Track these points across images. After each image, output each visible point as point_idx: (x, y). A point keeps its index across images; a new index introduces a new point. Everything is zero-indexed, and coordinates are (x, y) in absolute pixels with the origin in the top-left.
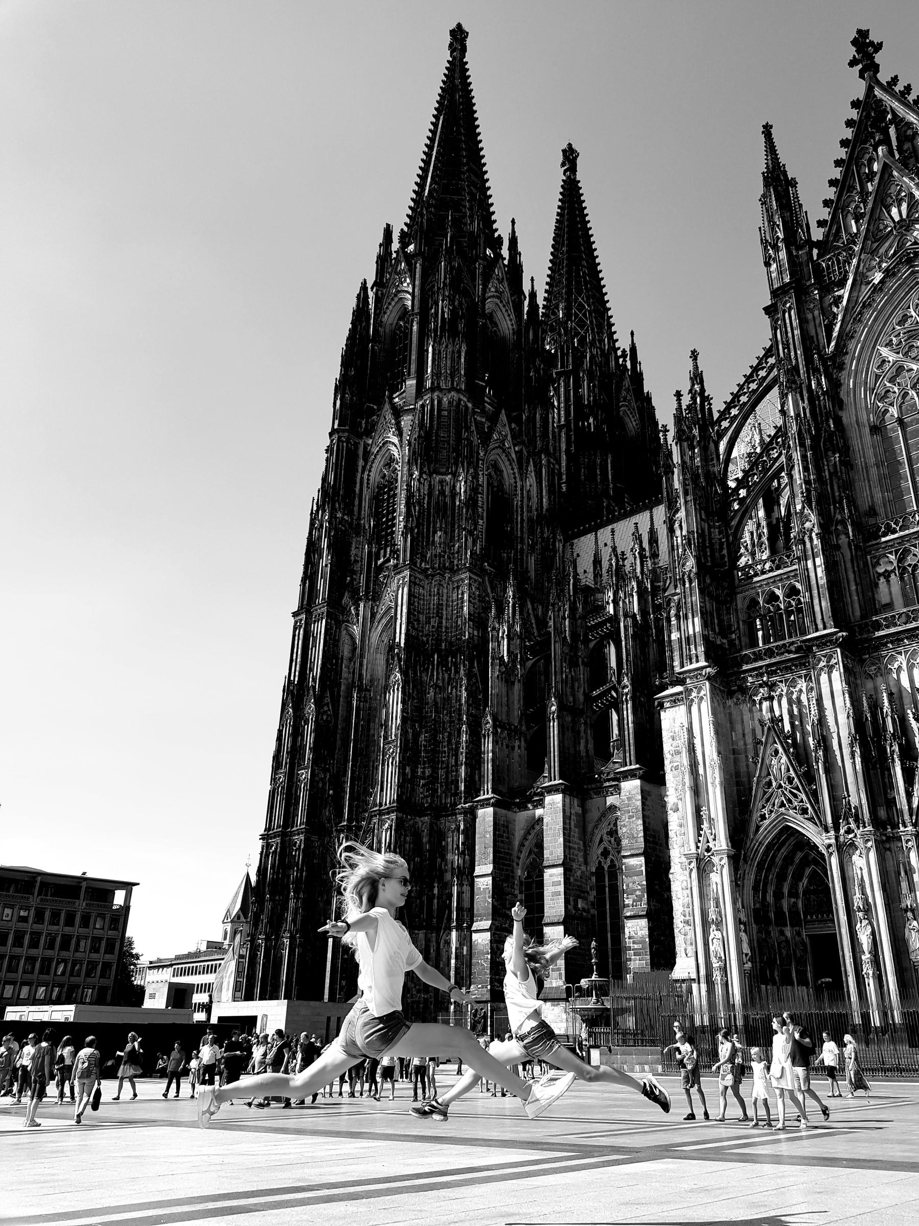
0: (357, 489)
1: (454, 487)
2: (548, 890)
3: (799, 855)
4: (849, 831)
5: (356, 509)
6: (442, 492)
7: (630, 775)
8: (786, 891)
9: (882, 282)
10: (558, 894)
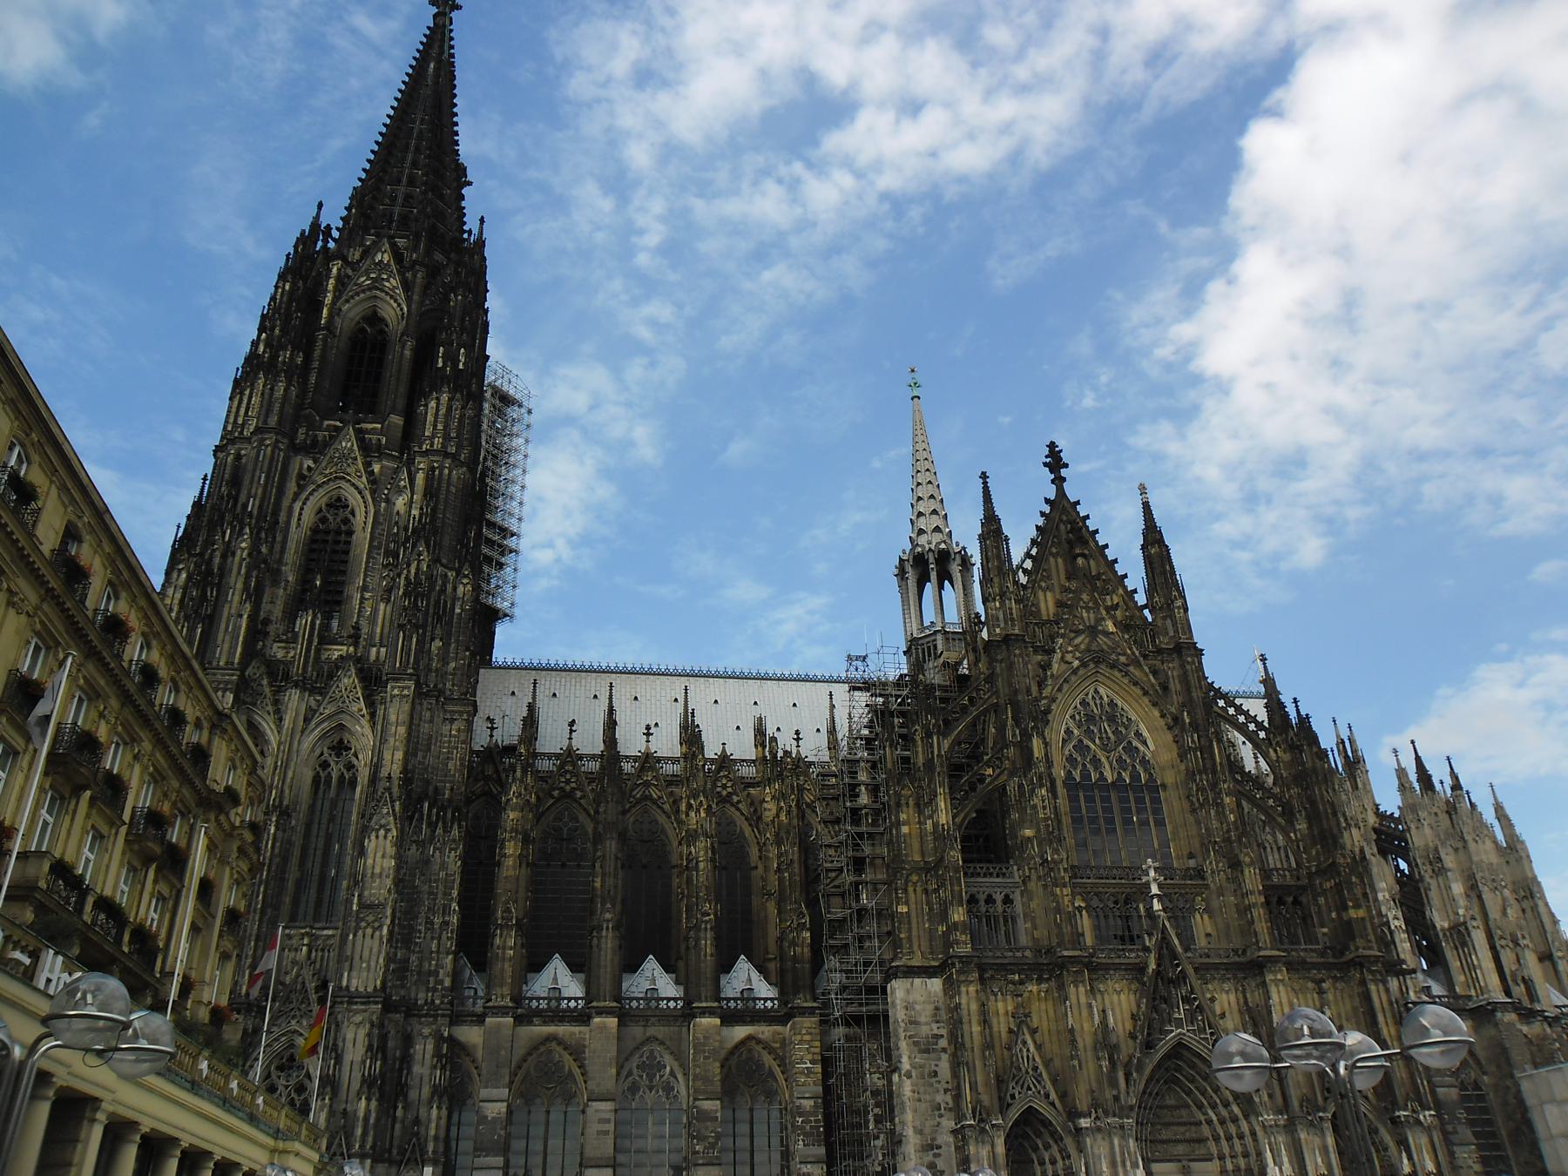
0: (282, 518)
1: (455, 589)
2: (593, 1128)
4: (1097, 1118)
5: (277, 547)
6: (443, 591)
7: (711, 1012)
10: (606, 1133)
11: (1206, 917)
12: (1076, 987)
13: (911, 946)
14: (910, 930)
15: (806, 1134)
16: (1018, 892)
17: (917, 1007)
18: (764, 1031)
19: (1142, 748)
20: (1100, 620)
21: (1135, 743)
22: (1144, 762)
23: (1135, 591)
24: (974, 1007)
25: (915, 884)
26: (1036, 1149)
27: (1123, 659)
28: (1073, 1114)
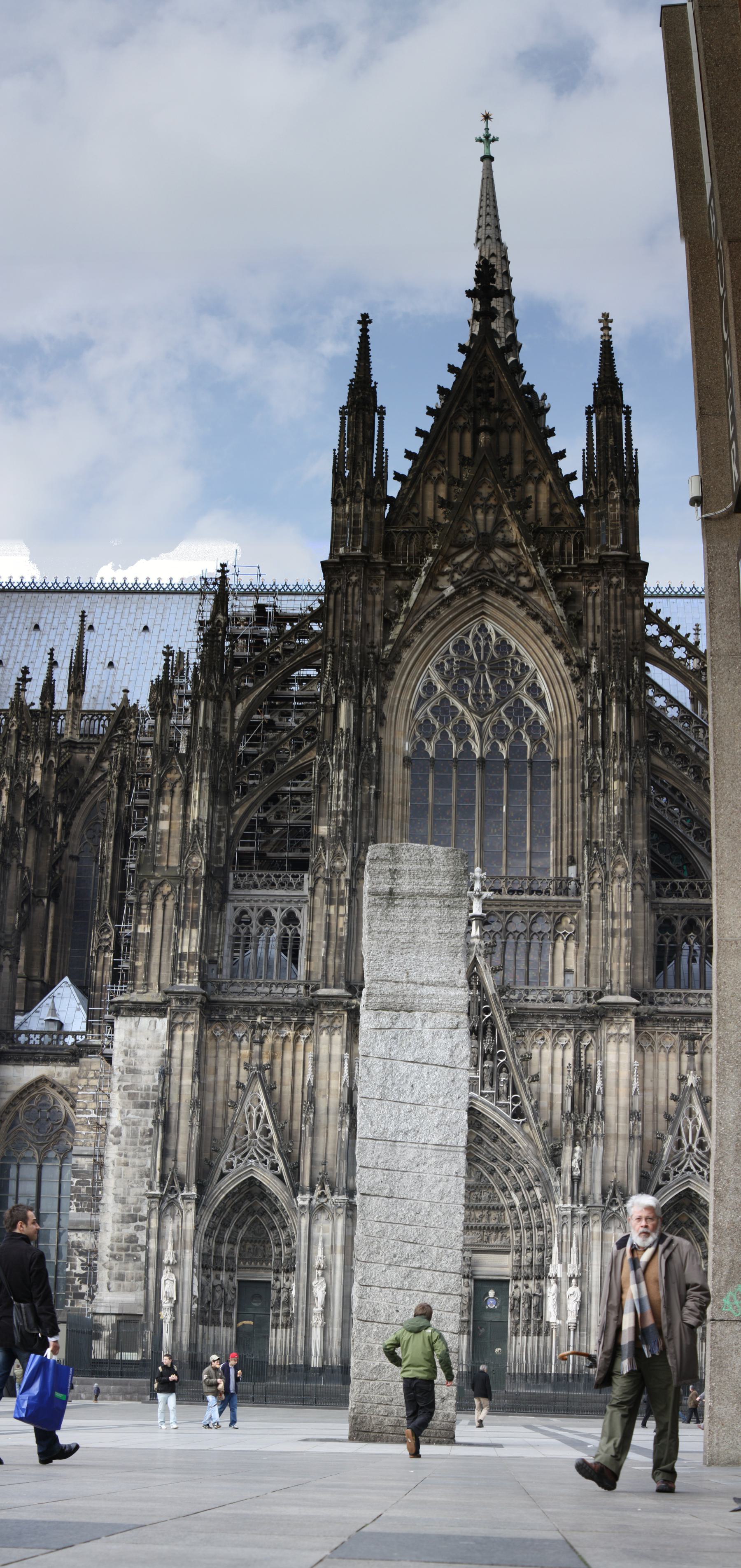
3: (247, 1204)
8: (227, 1236)
9: (452, 597)
11: (572, 945)
12: (331, 1035)
13: (147, 978)
14: (149, 958)
15: (80, 1198)
16: (305, 908)
17: (140, 1052)
18: (60, 1072)
19: (535, 708)
20: (500, 524)
21: (528, 702)
22: (535, 728)
23: (573, 477)
24: (189, 1054)
25: (165, 897)
26: (273, 1228)
27: (525, 581)
28: (296, 1190)
